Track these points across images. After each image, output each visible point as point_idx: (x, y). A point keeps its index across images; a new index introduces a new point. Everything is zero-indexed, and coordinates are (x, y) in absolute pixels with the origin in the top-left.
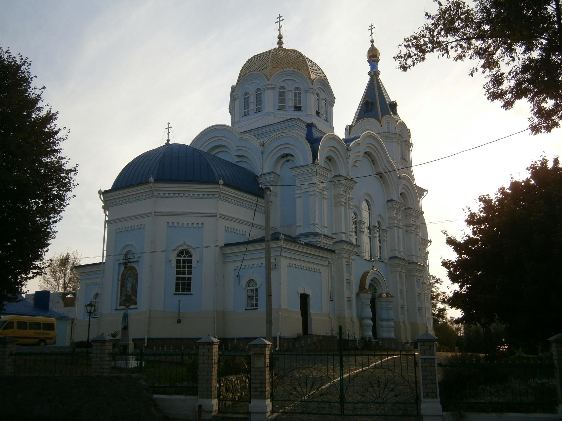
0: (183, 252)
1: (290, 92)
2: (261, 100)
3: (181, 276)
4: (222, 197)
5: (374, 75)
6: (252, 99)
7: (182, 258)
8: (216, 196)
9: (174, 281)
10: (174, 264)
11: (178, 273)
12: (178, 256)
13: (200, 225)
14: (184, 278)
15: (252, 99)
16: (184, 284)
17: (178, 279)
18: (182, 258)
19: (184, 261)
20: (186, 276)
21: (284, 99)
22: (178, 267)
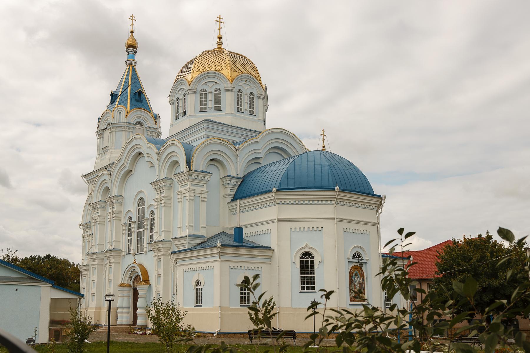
0: (304, 255)
1: (210, 94)
2: (220, 100)
3: (305, 275)
4: (339, 202)
5: (132, 66)
6: (210, 98)
7: (305, 260)
8: (333, 202)
9: (299, 281)
10: (298, 265)
11: (302, 273)
12: (302, 258)
13: (320, 229)
14: (307, 278)
15: (210, 98)
16: (308, 283)
17: (302, 278)
18: (305, 260)
19: (307, 262)
20: (310, 275)
21: (242, 102)
22: (302, 267)
